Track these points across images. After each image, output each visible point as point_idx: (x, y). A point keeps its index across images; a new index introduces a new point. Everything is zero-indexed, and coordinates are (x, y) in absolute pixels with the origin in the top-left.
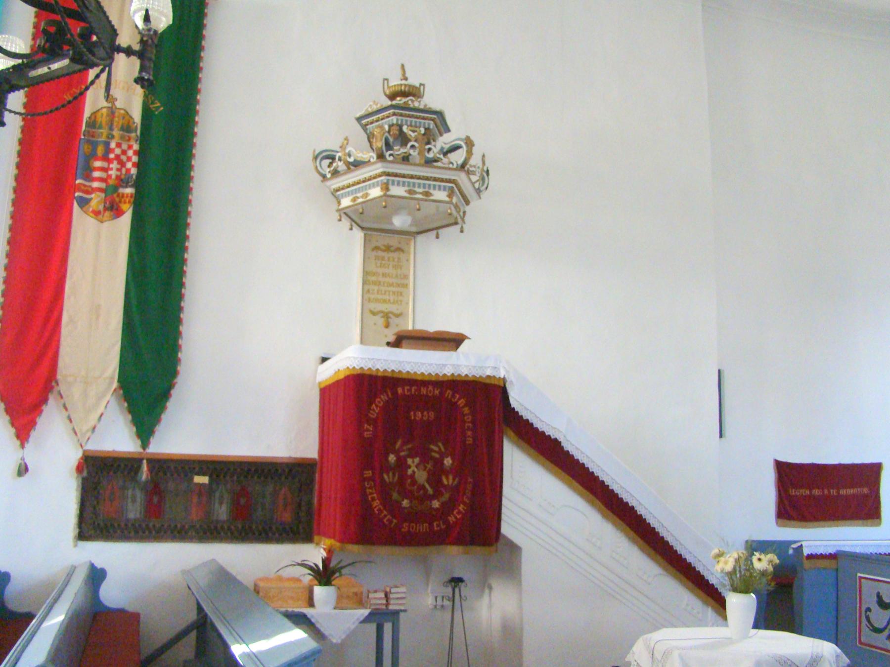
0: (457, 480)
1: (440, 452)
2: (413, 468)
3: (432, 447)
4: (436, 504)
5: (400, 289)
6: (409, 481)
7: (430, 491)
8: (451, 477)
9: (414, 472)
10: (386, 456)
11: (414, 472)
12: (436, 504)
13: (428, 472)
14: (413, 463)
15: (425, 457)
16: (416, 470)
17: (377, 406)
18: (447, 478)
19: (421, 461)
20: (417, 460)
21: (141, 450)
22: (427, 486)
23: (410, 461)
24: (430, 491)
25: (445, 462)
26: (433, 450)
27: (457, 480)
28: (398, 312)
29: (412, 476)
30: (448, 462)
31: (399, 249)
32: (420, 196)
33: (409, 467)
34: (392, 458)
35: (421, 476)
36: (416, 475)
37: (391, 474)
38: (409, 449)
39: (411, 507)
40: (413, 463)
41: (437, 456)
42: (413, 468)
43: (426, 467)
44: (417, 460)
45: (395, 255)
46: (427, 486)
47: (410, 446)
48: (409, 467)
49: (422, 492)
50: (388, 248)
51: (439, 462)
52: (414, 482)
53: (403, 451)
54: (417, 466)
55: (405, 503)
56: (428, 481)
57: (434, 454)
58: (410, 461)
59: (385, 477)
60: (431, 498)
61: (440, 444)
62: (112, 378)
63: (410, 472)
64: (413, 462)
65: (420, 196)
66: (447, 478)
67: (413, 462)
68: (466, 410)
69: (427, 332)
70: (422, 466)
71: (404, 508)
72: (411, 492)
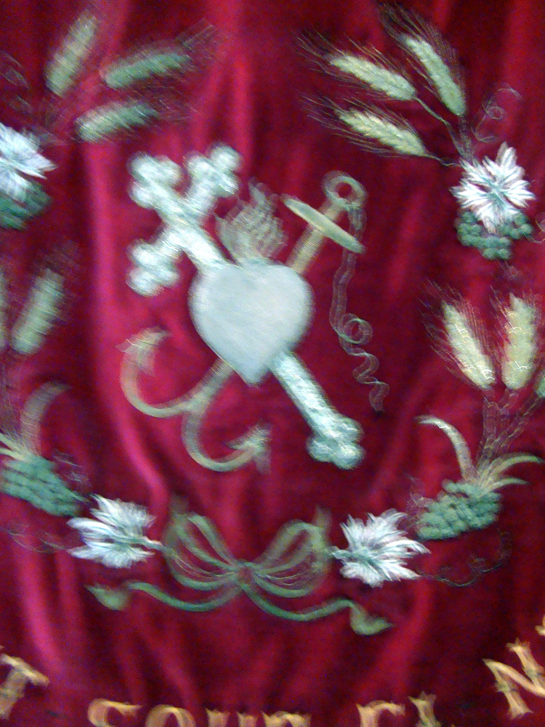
1: (420, 112)
2: (185, 237)
4: (381, 549)
6: (142, 346)
7: (336, 438)
8: (519, 318)
9: (187, 269)
11: (187, 269)
12: (381, 549)
13: (320, 277)
14: (181, 193)
16: (203, 252)
18: (493, 339)
19: (245, 175)
20: (217, 170)
22: (306, 393)
23: (152, 180)
24: (336, 438)
25: (469, 194)
26: (368, 99)
29: (175, 304)
33: (150, 225)
35: (256, 312)
36: (205, 302)
38: (144, 89)
39: (157, 569)
40: (181, 193)
41: (405, 141)
42: (185, 237)
43: (295, 229)
44: (217, 170)
46: (306, 393)
47: (158, 61)
48: (150, 225)
49: (253, 445)
51: (412, 204)
53: (106, 96)
54: (219, 216)
55: (113, 532)
56: (315, 349)
57: (369, 125)
58: (152, 180)
60: (345, 495)
61: (422, 49)
63: (151, 268)
64: (183, 186)
66: (493, 339)
67: (183, 186)
70: (255, 224)
71: (99, 572)
72: (159, 443)
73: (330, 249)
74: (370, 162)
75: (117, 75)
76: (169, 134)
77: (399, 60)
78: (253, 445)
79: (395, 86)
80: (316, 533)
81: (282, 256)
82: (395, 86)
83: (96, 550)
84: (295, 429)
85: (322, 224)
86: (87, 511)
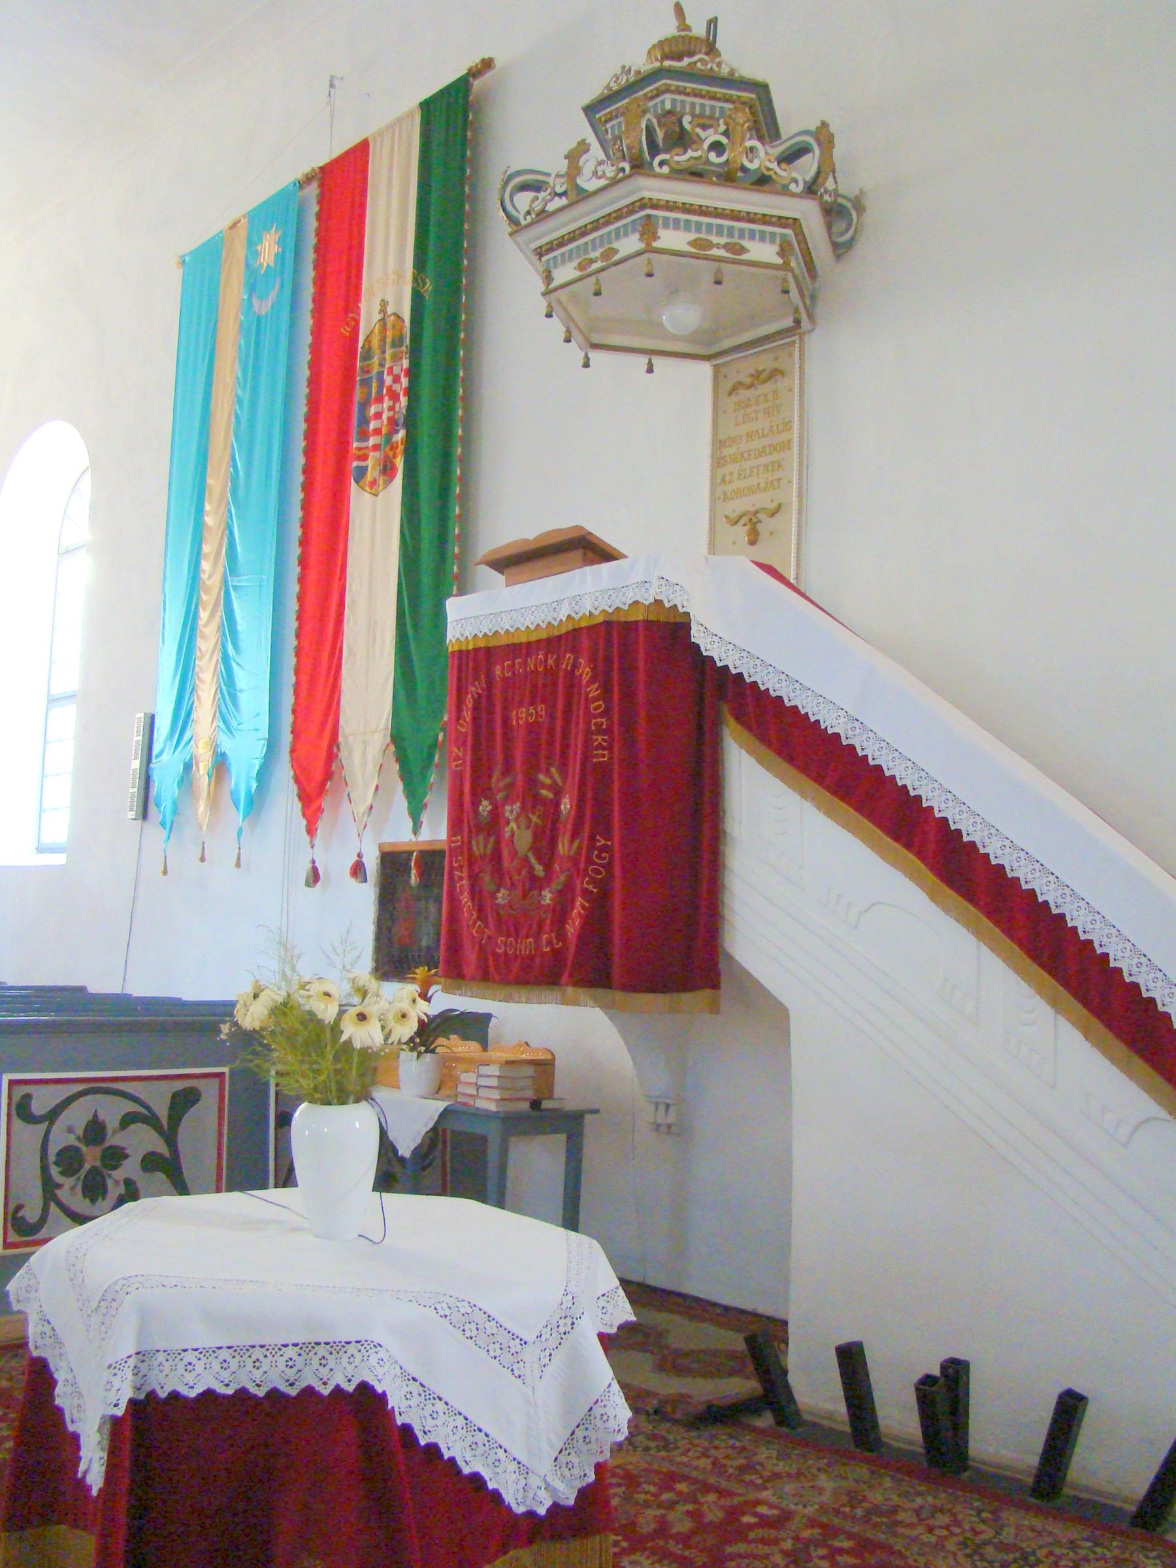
0: (576, 844)
2: (513, 825)
3: (541, 777)
5: (775, 457)
7: (539, 870)
10: (475, 804)
15: (531, 800)
17: (467, 709)
20: (517, 806)
21: (414, 839)
24: (539, 870)
26: (543, 786)
27: (576, 844)
28: (773, 506)
30: (566, 805)
31: (775, 373)
32: (722, 253)
33: (508, 822)
34: (485, 807)
37: (481, 839)
42: (513, 825)
45: (767, 388)
50: (759, 378)
52: (514, 854)
56: (534, 848)
57: (544, 792)
59: (473, 842)
62: (386, 729)
65: (722, 253)
68: (594, 691)
69: (526, 541)
73: (537, 825)
74: (544, 801)
75: (502, 784)
76: (508, 800)
77: (547, 772)
78: (524, 872)
79: (548, 781)
80: (535, 892)
81: (528, 827)
82: (548, 781)
83: (499, 901)
84: (531, 868)
85: (534, 819)
86: (498, 891)
